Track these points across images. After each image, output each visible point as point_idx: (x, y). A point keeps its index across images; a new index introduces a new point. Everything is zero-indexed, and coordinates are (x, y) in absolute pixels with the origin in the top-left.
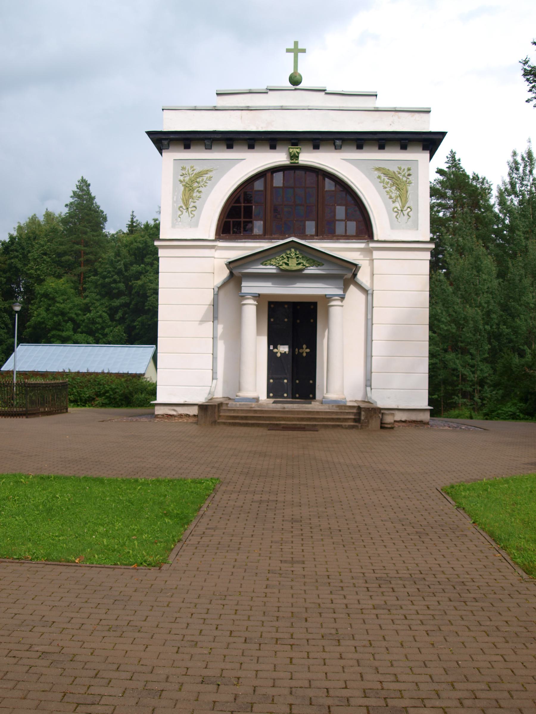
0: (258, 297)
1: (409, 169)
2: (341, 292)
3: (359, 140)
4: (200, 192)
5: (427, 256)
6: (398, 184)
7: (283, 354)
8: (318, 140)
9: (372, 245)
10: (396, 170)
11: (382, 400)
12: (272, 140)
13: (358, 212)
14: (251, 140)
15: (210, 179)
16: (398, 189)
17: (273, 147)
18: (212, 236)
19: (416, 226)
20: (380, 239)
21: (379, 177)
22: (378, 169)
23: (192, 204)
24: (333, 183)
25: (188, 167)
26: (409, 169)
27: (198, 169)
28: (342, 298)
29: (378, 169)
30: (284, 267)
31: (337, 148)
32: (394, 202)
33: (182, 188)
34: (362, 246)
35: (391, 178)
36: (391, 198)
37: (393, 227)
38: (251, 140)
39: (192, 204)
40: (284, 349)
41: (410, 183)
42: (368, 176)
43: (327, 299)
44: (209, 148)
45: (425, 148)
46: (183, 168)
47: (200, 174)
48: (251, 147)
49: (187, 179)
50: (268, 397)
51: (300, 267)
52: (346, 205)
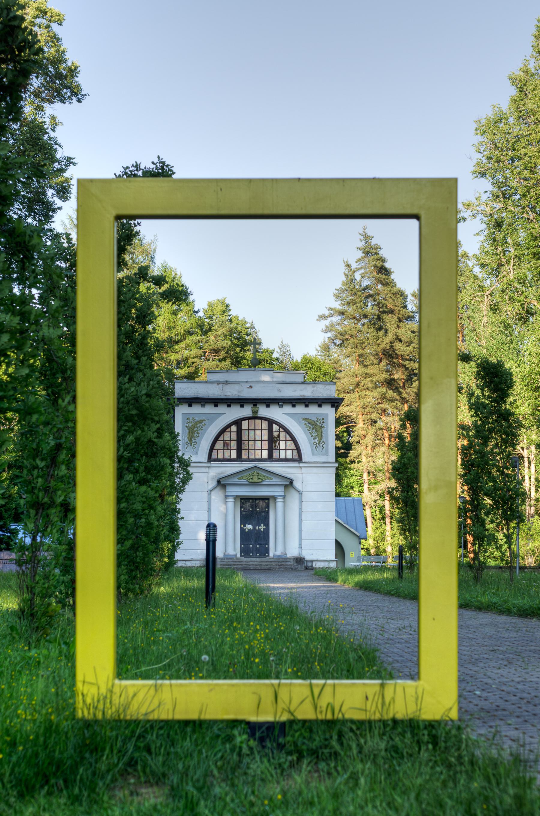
0: (236, 497)
1: (323, 419)
2: (283, 494)
3: (293, 402)
4: (198, 433)
5: (334, 471)
6: (316, 427)
7: (250, 530)
8: (268, 402)
9: (301, 465)
10: (315, 419)
11: (308, 555)
12: (242, 402)
13: (293, 445)
14: (229, 402)
15: (204, 425)
16: (316, 431)
17: (242, 406)
18: (206, 461)
19: (327, 453)
20: (307, 461)
21: (305, 424)
22: (305, 419)
23: (194, 441)
24: (278, 427)
25: (191, 418)
26: (323, 419)
27: (197, 419)
28: (284, 497)
29: (305, 419)
30: (251, 480)
31: (281, 406)
32: (314, 439)
33: (187, 431)
34: (297, 465)
35: (311, 424)
36: (312, 436)
37: (313, 454)
38: (229, 402)
39: (194, 441)
40: (250, 527)
41: (324, 427)
42: (299, 423)
43: (274, 498)
44: (203, 406)
45: (332, 406)
46: (188, 419)
47: (199, 422)
48: (229, 406)
49: (190, 425)
50: (241, 556)
51: (260, 480)
52: (286, 441)
